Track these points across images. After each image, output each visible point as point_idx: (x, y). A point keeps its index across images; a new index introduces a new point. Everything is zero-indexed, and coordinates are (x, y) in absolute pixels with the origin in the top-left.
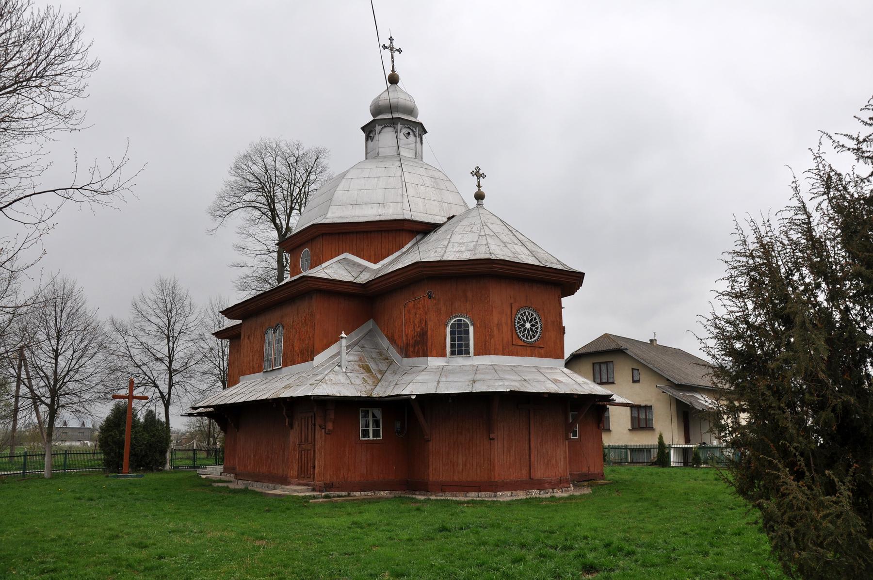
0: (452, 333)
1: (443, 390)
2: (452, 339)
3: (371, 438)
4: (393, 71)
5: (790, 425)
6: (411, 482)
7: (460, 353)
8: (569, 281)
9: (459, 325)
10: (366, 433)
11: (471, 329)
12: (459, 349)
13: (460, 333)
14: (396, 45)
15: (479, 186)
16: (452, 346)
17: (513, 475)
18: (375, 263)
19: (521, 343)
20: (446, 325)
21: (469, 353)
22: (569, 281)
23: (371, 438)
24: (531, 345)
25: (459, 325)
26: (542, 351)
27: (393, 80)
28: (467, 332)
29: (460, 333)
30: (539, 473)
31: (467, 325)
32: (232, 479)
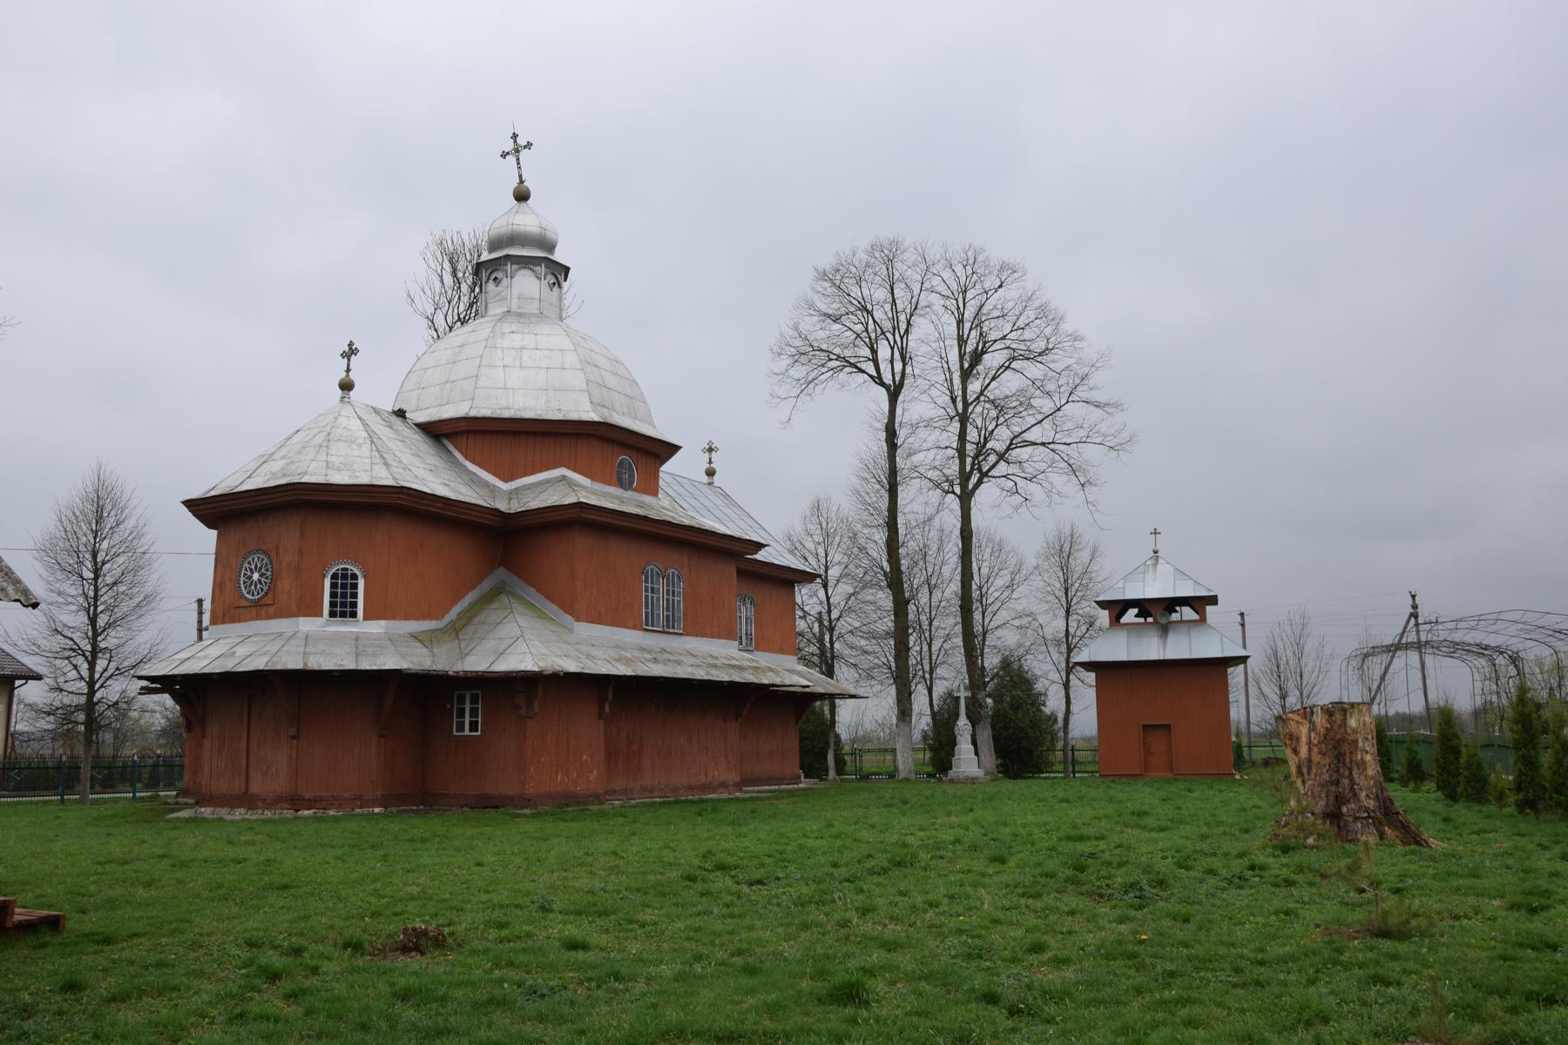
0: (333, 586)
1: (366, 665)
2: (333, 595)
3: (467, 732)
4: (522, 182)
5: (1368, 757)
6: (417, 792)
7: (343, 615)
8: (674, 449)
9: (344, 577)
10: (461, 727)
11: (361, 583)
12: (343, 609)
13: (344, 585)
14: (509, 146)
15: (348, 370)
16: (333, 604)
17: (223, 787)
18: (506, 480)
19: (245, 603)
20: (324, 576)
21: (354, 615)
22: (674, 449)
23: (467, 732)
24: (257, 604)
25: (344, 577)
26: (271, 610)
27: (522, 196)
28: (355, 586)
29: (344, 585)
30: (255, 788)
31: (355, 577)
32: (592, 780)
